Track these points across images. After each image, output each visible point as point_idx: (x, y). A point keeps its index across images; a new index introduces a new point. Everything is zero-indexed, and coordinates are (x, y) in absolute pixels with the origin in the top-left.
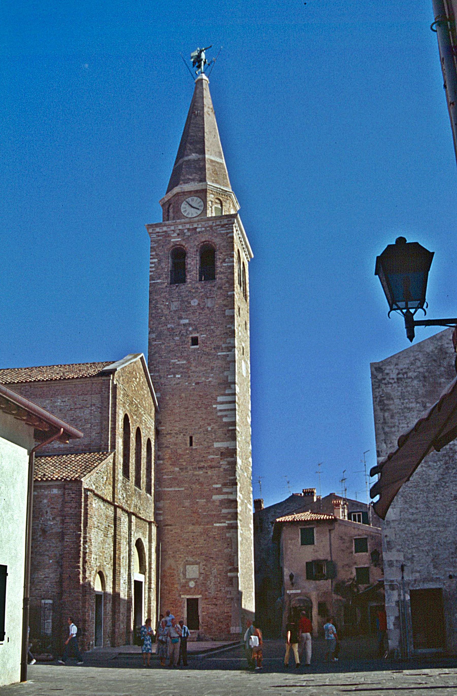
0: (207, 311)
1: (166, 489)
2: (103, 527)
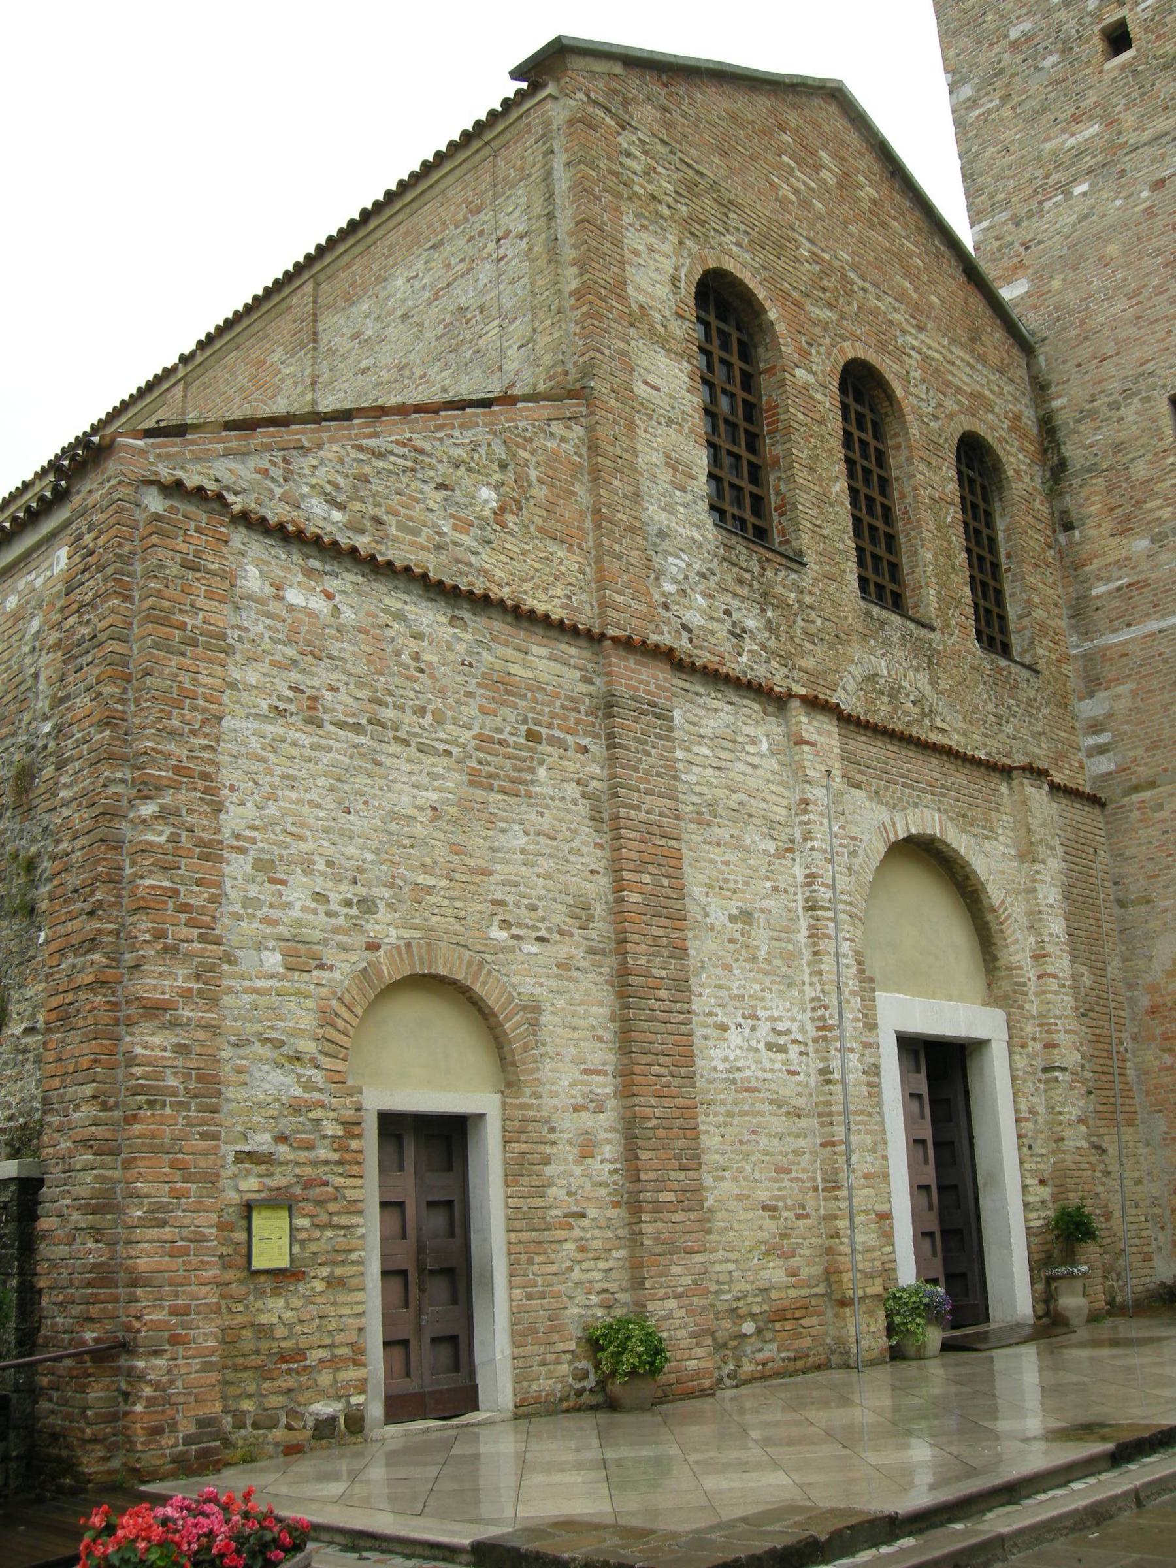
1: (1113, 639)
2: (465, 736)
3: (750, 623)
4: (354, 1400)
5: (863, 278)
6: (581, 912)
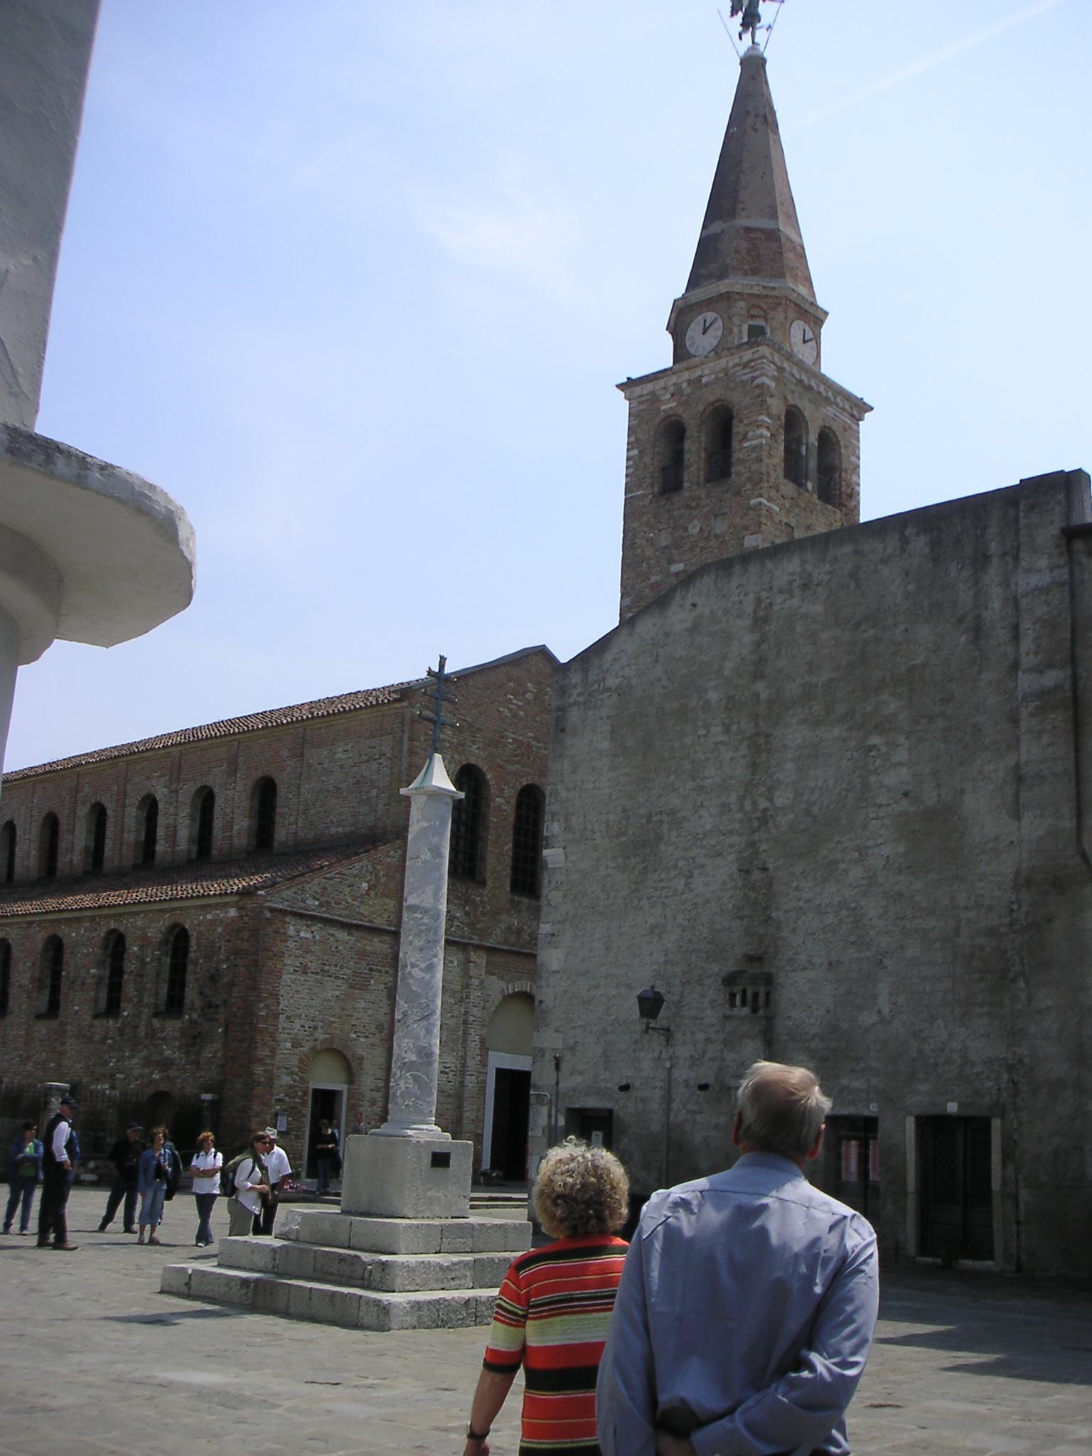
0: (713, 543)
2: (349, 972)
3: (458, 915)
4: (299, 1169)
5: (539, 742)
6: (380, 1027)
